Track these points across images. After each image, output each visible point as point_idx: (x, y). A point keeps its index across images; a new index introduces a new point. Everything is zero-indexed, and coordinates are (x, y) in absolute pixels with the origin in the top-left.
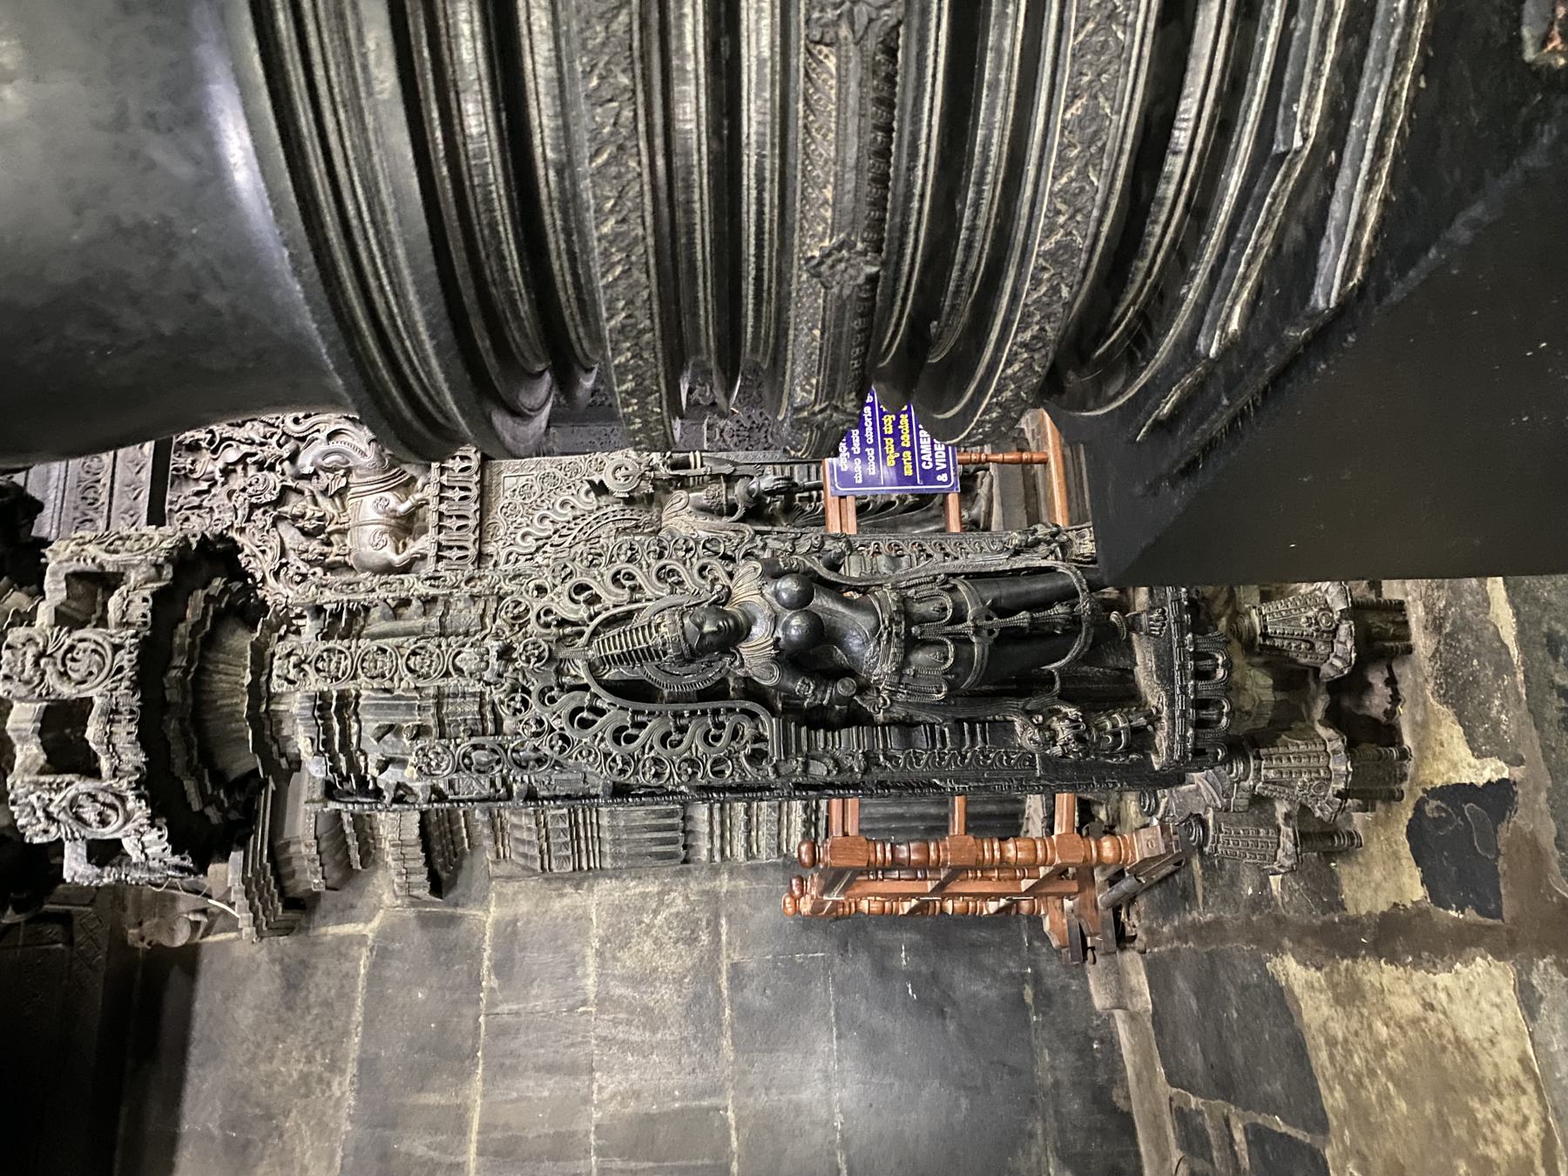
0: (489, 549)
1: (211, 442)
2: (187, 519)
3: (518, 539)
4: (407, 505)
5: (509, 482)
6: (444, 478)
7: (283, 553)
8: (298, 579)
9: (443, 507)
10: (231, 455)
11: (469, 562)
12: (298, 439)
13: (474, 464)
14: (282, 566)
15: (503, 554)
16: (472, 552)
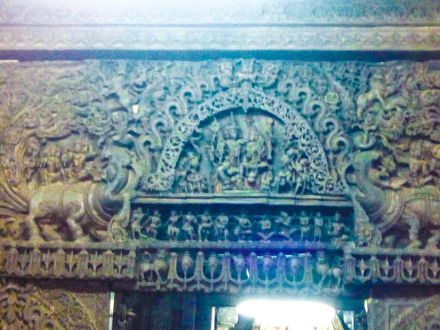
14: (39, 139)
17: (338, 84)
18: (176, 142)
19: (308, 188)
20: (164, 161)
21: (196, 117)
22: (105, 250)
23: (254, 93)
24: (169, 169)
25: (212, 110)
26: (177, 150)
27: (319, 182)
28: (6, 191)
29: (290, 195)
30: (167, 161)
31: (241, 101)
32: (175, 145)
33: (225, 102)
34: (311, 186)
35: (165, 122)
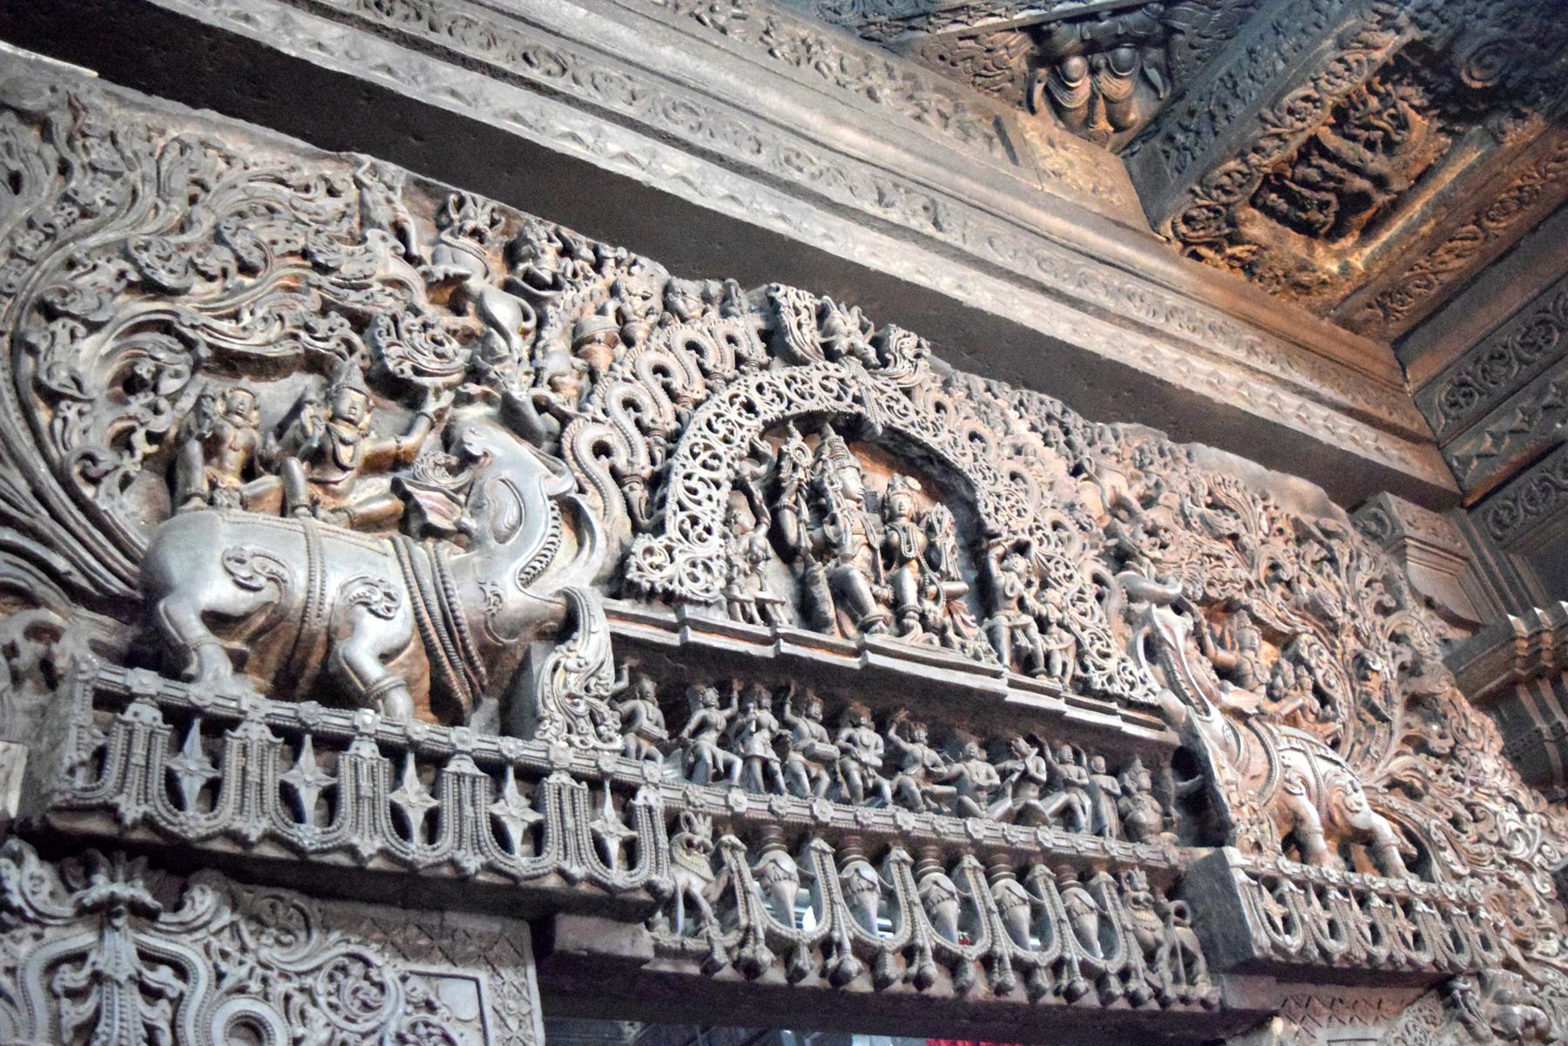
0: (204, 901)
1: (529, 277)
2: (332, 192)
3: (240, 1005)
4: (373, 670)
5: (458, 999)
6: (469, 767)
7: (231, 363)
8: (144, 370)
9: (366, 750)
10: (505, 309)
11: (158, 807)
12: (558, 440)
13: (521, 861)
14: (190, 345)
15: (186, 949)
16: (194, 823)
17: (1035, 440)
18: (711, 462)
19: (1079, 672)
20: (682, 508)
21: (750, 407)
22: (547, 773)
23: (883, 392)
24: (705, 535)
25: (790, 402)
26: (718, 485)
27: (1100, 661)
28: (39, 495)
29: (1042, 681)
30: (695, 510)
31: (857, 400)
32: (705, 465)
33: (817, 390)
34: (1085, 669)
35: (644, 400)
